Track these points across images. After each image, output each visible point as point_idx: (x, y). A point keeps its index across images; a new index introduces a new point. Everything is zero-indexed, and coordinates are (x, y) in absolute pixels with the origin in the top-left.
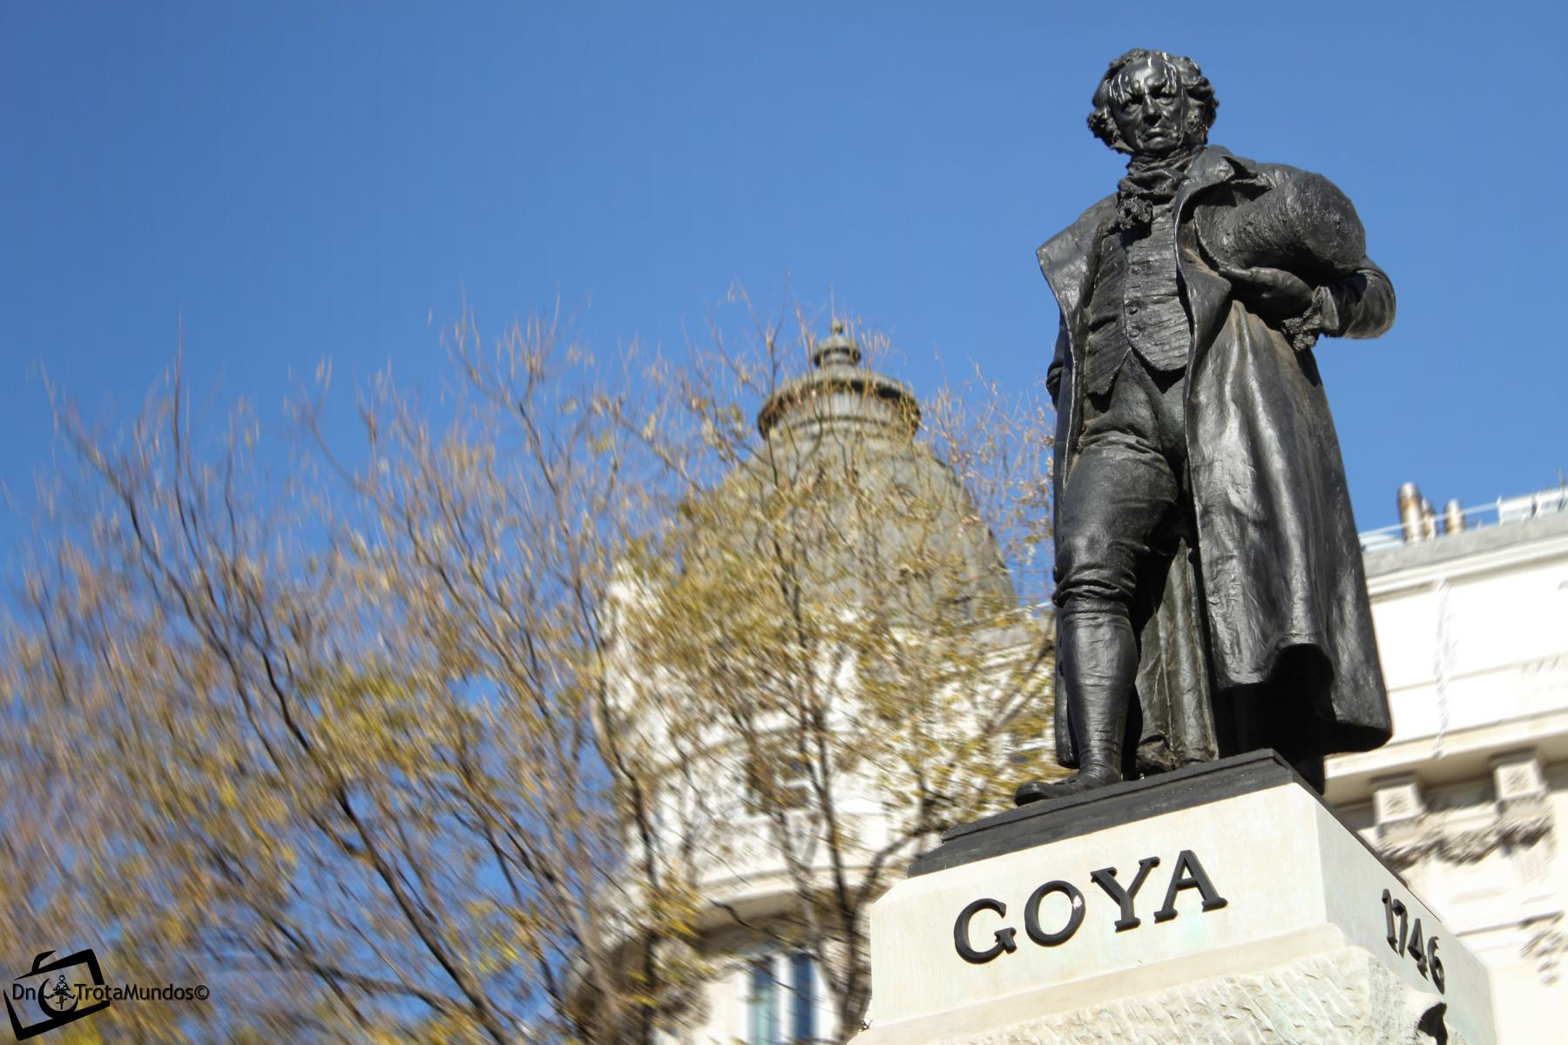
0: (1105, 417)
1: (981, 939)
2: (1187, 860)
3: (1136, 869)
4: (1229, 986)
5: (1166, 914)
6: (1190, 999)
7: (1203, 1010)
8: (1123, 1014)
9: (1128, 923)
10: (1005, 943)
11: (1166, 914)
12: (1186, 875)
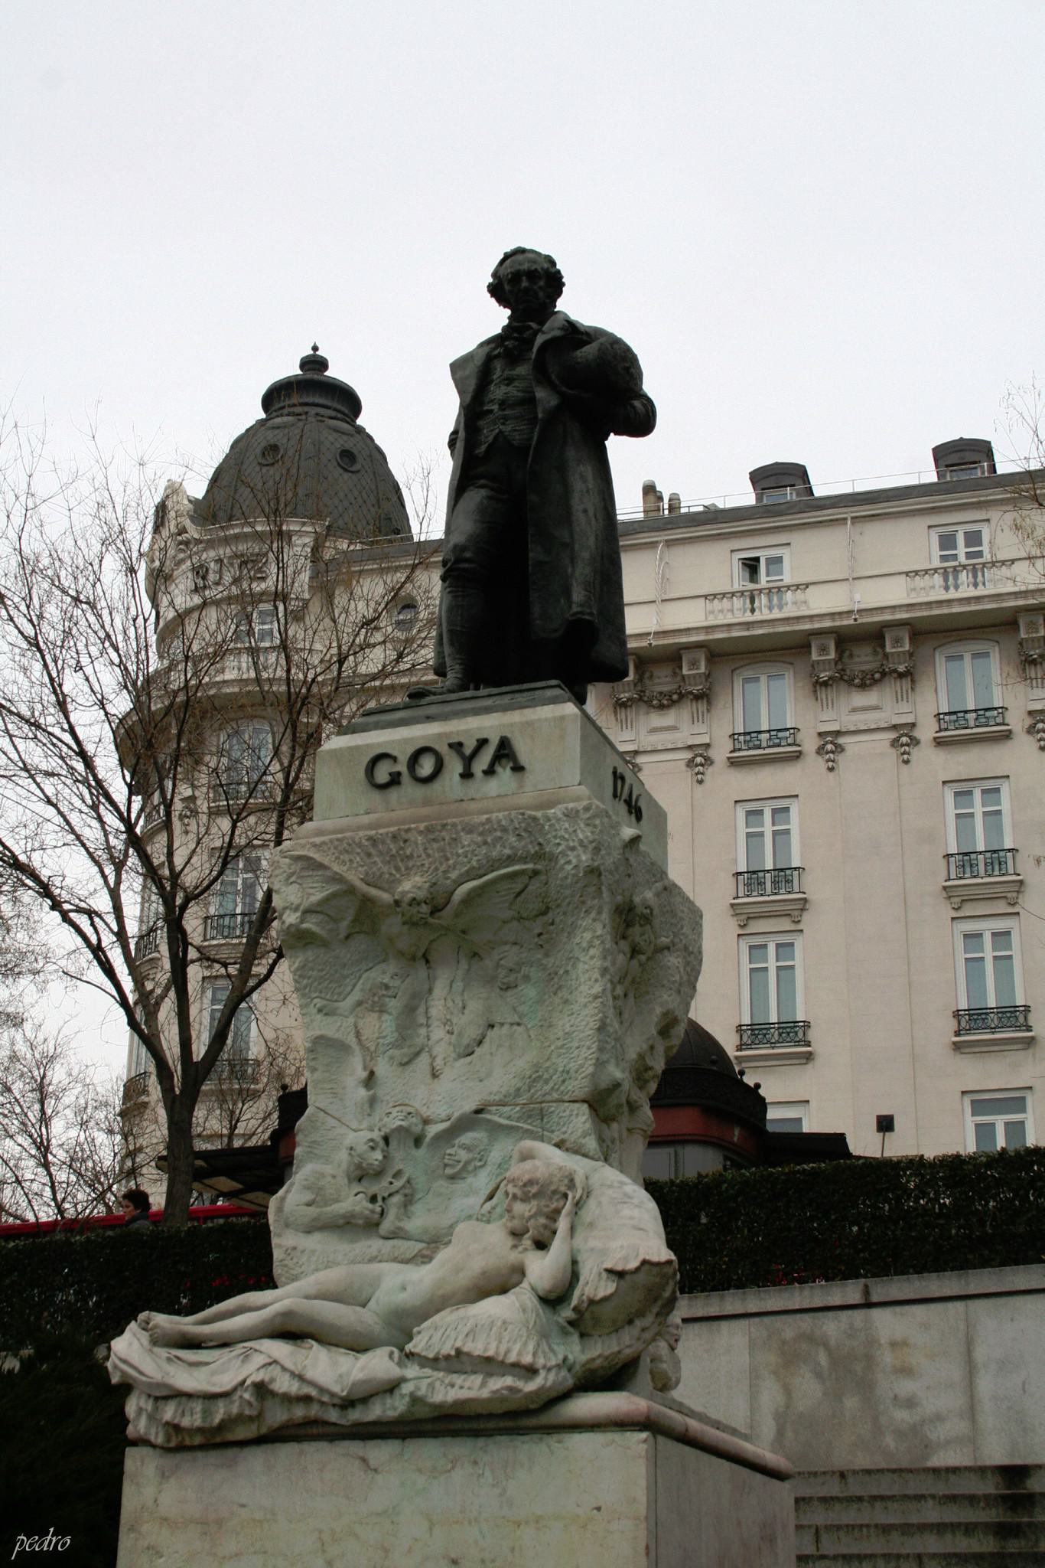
1: (382, 774)
3: (475, 743)
5: (490, 772)
7: (504, 830)
10: (395, 780)
11: (490, 772)
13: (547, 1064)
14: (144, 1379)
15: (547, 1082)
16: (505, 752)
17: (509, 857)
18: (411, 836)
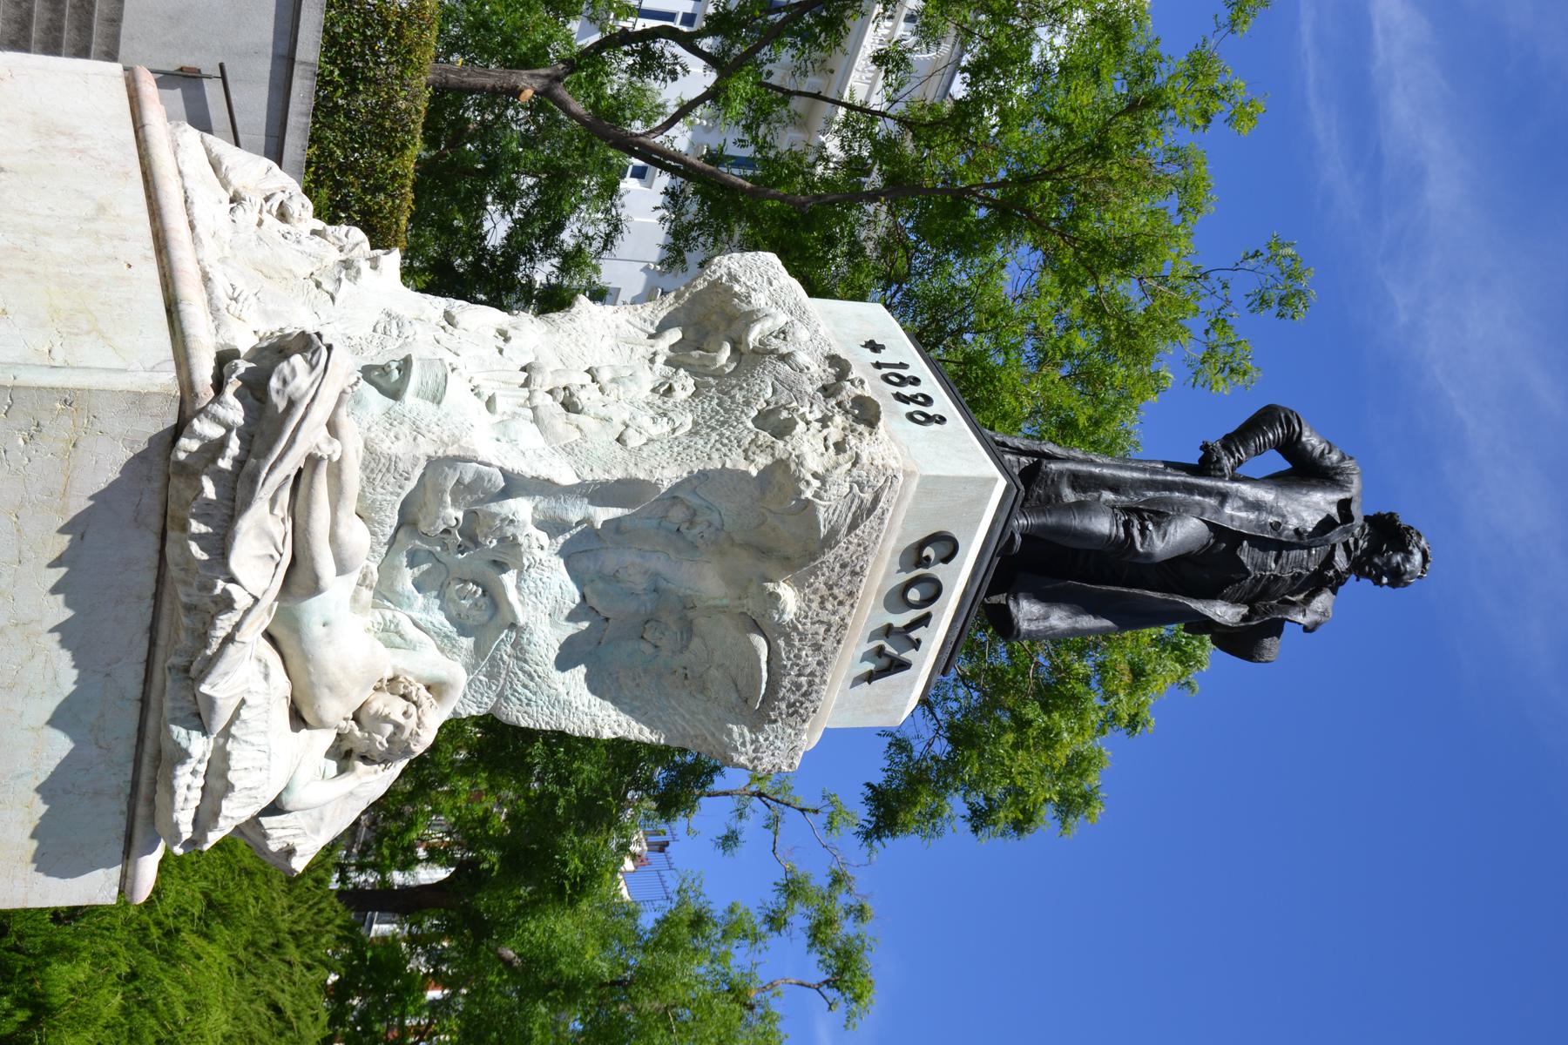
2: (904, 665)
13: (544, 686)
14: (263, 474)
15: (525, 686)
18: (844, 610)
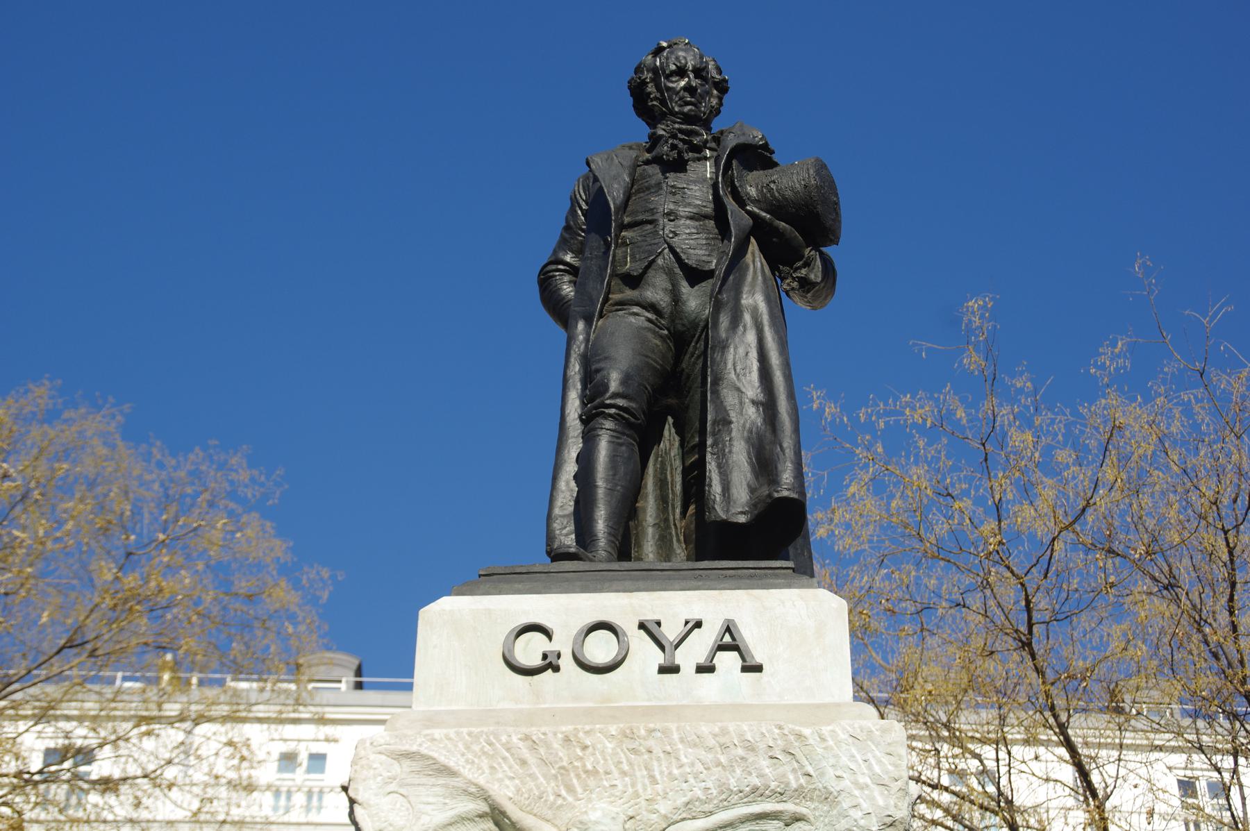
0: (629, 294)
4: (777, 731)
6: (741, 735)
7: (751, 748)
8: (676, 736)
9: (669, 669)
10: (550, 664)
12: (727, 639)
16: (730, 641)
17: (755, 790)
